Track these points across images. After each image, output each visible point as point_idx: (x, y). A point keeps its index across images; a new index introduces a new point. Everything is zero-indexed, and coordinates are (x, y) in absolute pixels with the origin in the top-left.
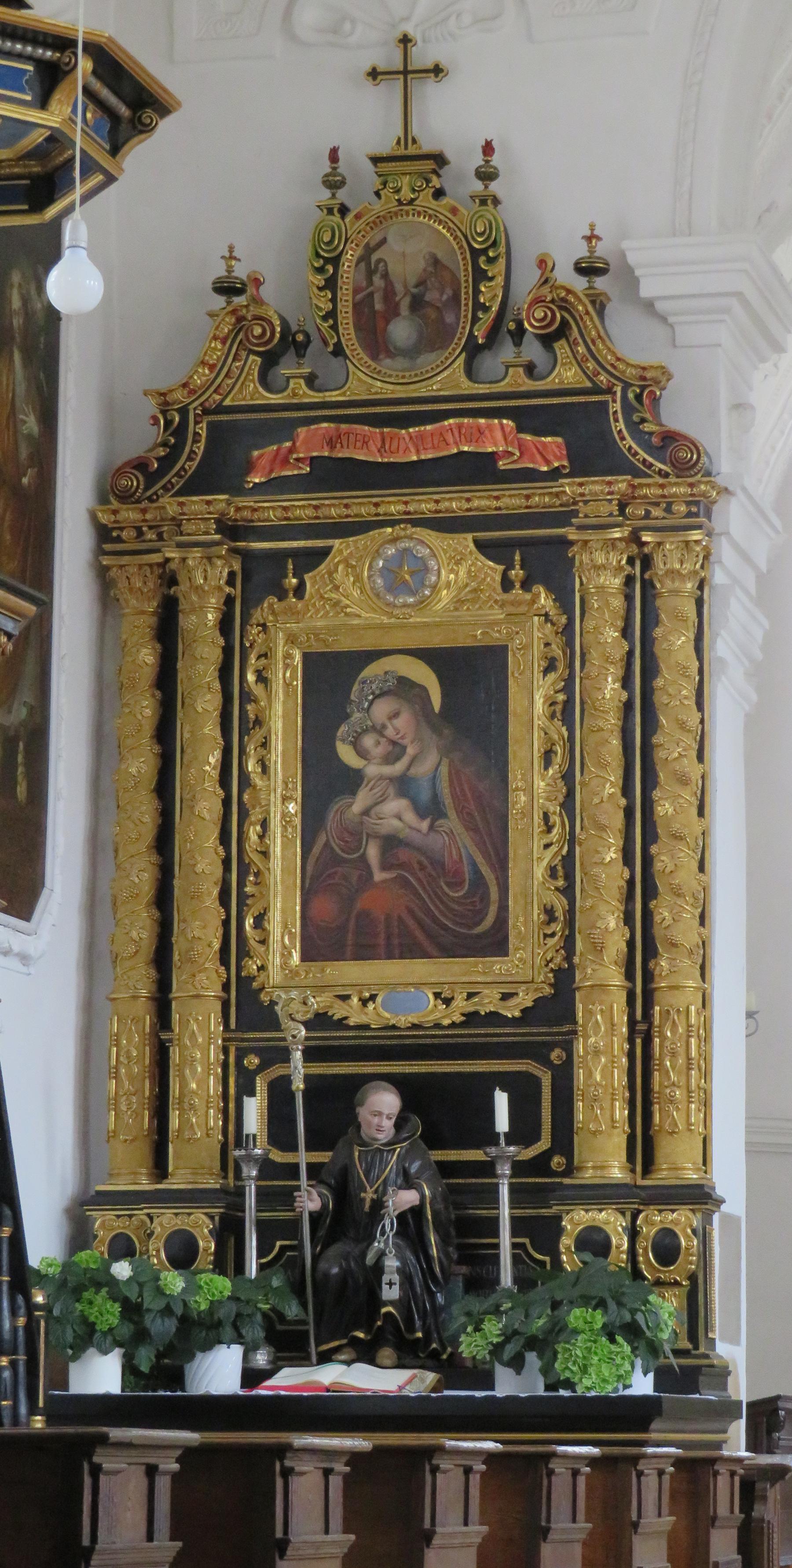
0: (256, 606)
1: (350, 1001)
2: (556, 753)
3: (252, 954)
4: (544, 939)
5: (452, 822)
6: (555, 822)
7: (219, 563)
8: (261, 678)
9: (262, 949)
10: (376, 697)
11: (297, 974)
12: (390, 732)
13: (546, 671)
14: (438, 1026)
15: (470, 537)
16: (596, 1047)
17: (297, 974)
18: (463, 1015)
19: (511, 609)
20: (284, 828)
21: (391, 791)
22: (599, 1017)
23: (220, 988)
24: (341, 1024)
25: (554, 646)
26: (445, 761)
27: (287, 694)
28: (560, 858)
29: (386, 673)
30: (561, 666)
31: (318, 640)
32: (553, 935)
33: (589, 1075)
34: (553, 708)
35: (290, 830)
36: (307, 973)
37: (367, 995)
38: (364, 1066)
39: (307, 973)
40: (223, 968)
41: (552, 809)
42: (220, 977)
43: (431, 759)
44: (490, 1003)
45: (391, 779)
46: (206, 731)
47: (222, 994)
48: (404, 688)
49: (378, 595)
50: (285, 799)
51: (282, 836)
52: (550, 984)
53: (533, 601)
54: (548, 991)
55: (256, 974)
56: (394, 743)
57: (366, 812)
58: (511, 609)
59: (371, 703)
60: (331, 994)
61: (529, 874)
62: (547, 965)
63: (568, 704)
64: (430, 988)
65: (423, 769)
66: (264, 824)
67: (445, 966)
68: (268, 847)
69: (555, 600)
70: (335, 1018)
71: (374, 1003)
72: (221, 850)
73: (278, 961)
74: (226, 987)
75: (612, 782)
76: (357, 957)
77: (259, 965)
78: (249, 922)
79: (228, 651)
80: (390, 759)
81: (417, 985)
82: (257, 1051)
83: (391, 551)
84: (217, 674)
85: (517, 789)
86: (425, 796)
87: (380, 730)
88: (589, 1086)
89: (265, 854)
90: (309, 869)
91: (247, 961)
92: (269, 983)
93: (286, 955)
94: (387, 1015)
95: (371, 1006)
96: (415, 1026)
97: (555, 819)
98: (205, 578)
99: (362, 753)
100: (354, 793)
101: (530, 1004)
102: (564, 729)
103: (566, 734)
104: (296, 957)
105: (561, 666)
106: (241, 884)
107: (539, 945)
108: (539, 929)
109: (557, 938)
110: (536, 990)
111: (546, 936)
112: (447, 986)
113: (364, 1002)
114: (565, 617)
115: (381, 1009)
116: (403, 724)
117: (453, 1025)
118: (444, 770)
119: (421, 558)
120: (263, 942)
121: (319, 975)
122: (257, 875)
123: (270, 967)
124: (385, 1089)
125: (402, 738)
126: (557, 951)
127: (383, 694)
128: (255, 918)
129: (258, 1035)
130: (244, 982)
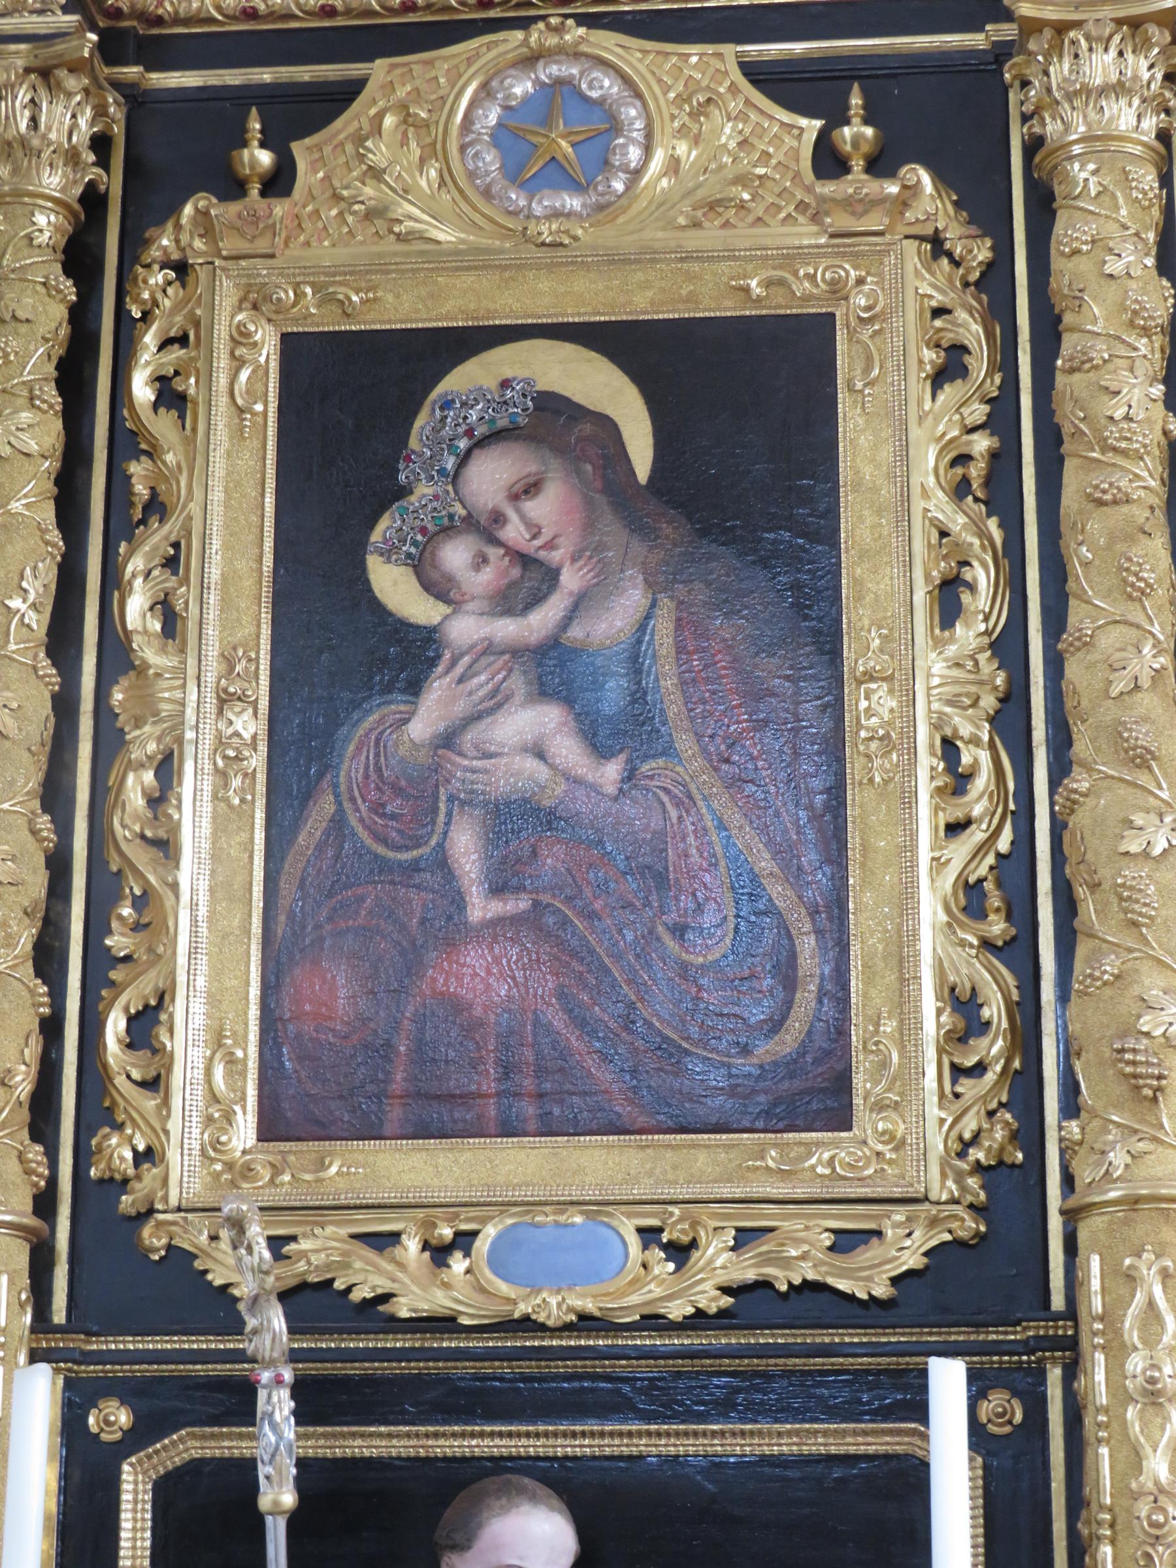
0: (161, 222)
1: (397, 1251)
2: (972, 587)
3: (121, 1117)
4: (954, 1082)
5: (689, 760)
6: (976, 764)
7: (72, 83)
8: (170, 396)
9: (149, 1103)
10: (481, 443)
11: (247, 1171)
12: (514, 532)
13: (939, 378)
14: (652, 1321)
15: (730, 50)
16: (1152, 1381)
17: (247, 1171)
18: (726, 1290)
19: (840, 220)
20: (222, 776)
21: (517, 684)
22: (1158, 1291)
23: (29, 1208)
24: (373, 1312)
25: (962, 315)
26: (666, 605)
27: (238, 433)
28: (990, 860)
29: (505, 384)
30: (979, 364)
31: (326, 299)
32: (980, 1069)
33: (1136, 1462)
34: (959, 471)
35: (236, 782)
36: (276, 1171)
37: (447, 1232)
38: (436, 1435)
39: (276, 1171)
40: (39, 1148)
41: (966, 730)
42: (28, 1172)
43: (632, 599)
44: (804, 1257)
45: (516, 652)
46: (16, 506)
47: (31, 1221)
48: (553, 421)
49: (487, 194)
50: (224, 700)
51: (215, 797)
52: (971, 1206)
53: (903, 203)
54: (969, 1226)
55: (131, 1172)
56: (525, 560)
57: (448, 740)
58: (840, 220)
59: (465, 459)
60: (344, 1231)
61: (905, 902)
62: (962, 1155)
63: (1004, 461)
64: (629, 1216)
65: (613, 622)
66: (167, 768)
67: (669, 1154)
68: (176, 828)
69: (956, 204)
70: (356, 1296)
71: (467, 1254)
72: (44, 821)
73: (196, 1135)
74: (45, 1204)
75: (1157, 643)
76: (422, 1131)
77: (141, 1147)
78: (115, 1025)
79: (81, 319)
80: (512, 601)
81: (598, 1208)
82: (127, 1391)
83: (521, 87)
84: (50, 369)
85: (870, 676)
86: (613, 694)
87: (486, 527)
88: (1136, 1496)
89: (166, 847)
90: (287, 887)
91: (106, 1137)
92: (165, 1199)
93: (219, 1117)
94: (504, 1288)
95: (458, 1264)
96: (586, 1322)
97: (976, 756)
98: (34, 121)
99: (437, 586)
100: (415, 688)
101: (912, 1260)
102: (993, 524)
103: (997, 535)
104: (244, 1132)
105: (979, 364)
106: (96, 928)
107: (942, 1095)
108: (940, 1051)
109: (990, 1077)
110: (933, 1222)
111: (958, 1071)
112: (676, 1210)
113: (439, 1253)
114: (988, 243)
115: (488, 1273)
116: (551, 512)
117: (699, 1320)
118: (663, 629)
119: (600, 103)
120: (153, 1084)
121: (308, 1177)
122: (140, 903)
123: (173, 1155)
124: (534, 1499)
125: (550, 545)
126: (991, 1114)
127: (495, 436)
128: (130, 1019)
129: (130, 1344)
130: (96, 1192)
